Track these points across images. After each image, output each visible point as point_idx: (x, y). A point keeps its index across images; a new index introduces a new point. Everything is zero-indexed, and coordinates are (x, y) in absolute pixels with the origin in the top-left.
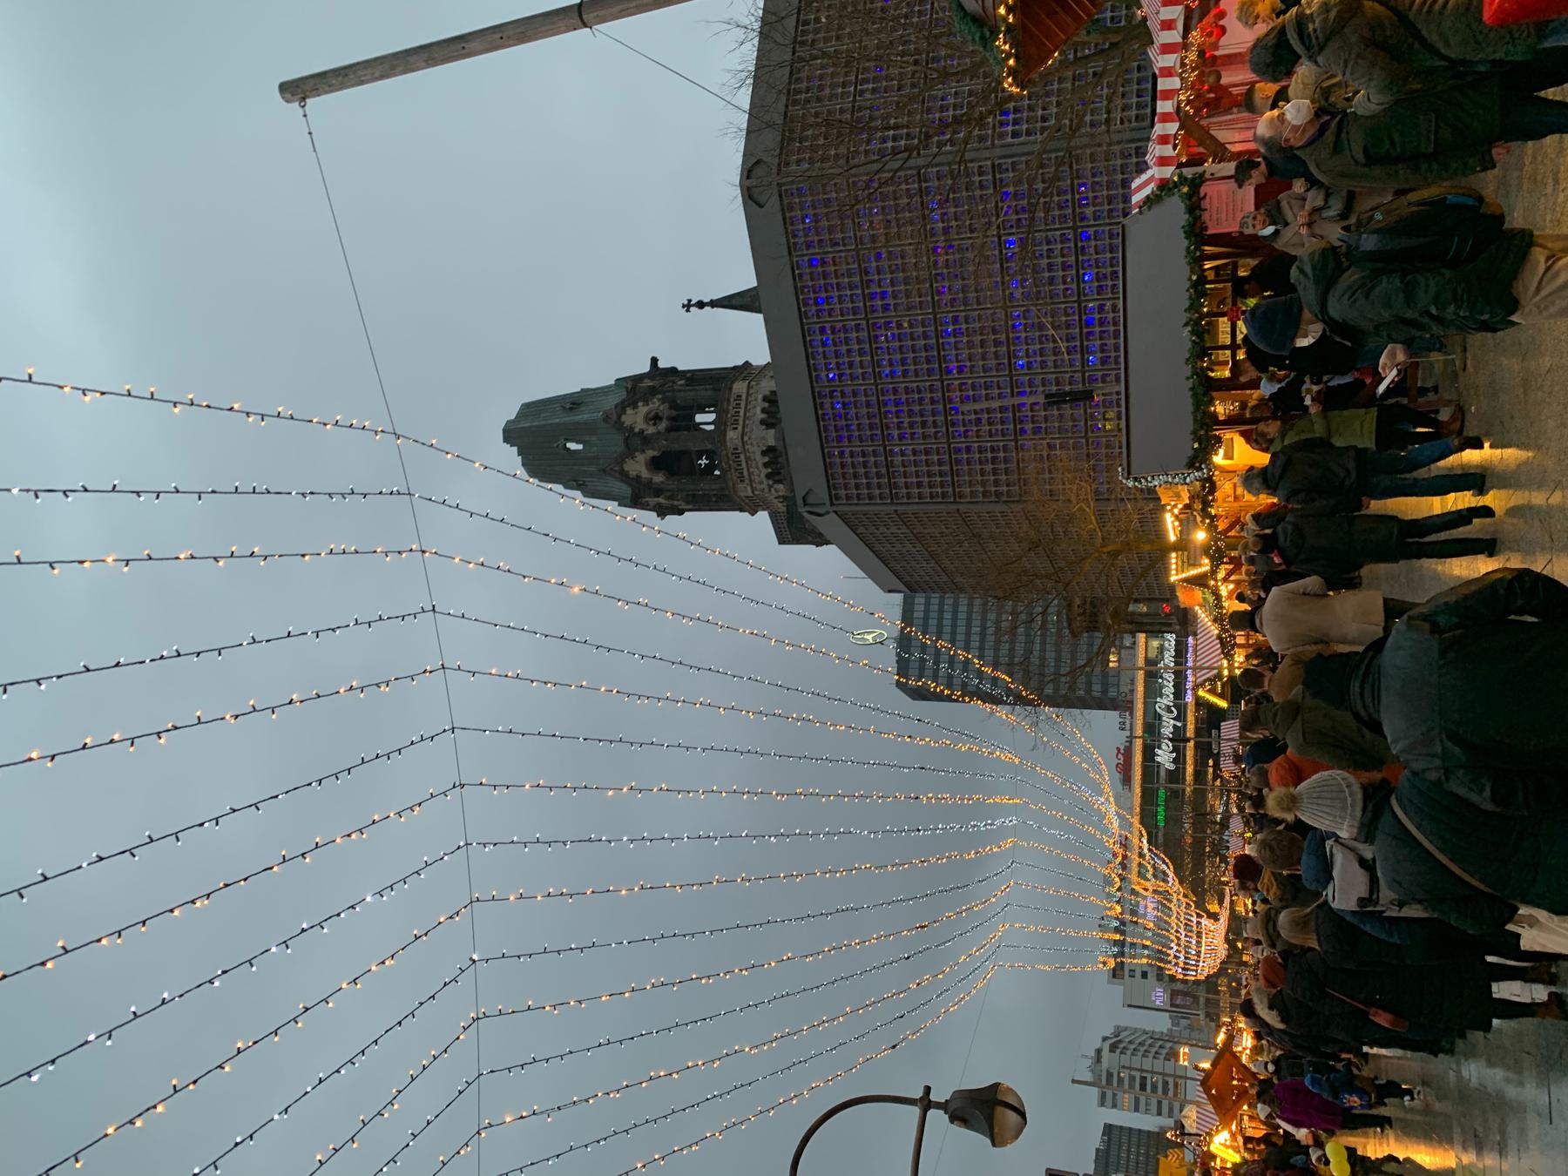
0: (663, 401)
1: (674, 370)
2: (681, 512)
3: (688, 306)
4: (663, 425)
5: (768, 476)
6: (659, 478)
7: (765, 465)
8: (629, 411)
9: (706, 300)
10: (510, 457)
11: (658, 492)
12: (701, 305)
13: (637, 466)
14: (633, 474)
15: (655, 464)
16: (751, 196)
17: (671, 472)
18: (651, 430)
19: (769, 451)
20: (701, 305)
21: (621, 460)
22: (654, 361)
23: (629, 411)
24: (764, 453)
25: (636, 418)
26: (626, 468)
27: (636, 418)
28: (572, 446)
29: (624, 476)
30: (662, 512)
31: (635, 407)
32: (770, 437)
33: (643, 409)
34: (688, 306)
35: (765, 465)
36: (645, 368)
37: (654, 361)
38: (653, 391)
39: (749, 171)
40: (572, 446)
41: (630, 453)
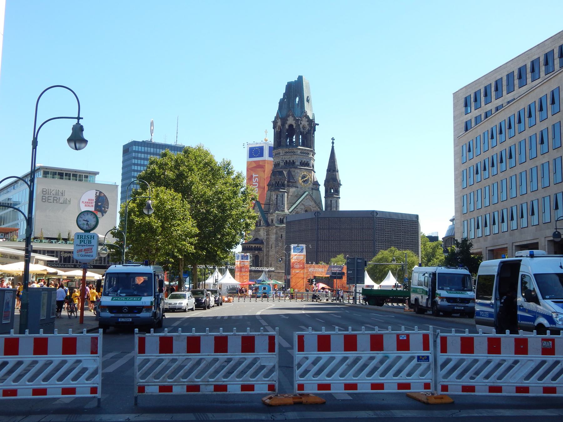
0: (308, 130)
1: (314, 130)
2: (274, 128)
3: (333, 139)
4: (302, 130)
5: (286, 161)
6: (287, 127)
7: (290, 161)
8: (307, 119)
9: (334, 145)
10: (294, 78)
11: (283, 124)
12: (333, 143)
13: (291, 121)
14: (288, 118)
15: (291, 126)
16: (373, 212)
17: (287, 131)
18: (301, 126)
19: (294, 163)
20: (333, 143)
21: (293, 116)
22: (318, 125)
23: (307, 119)
24: (293, 161)
25: (304, 122)
26: (291, 117)
27: (304, 122)
28: (297, 99)
29: (288, 116)
30: (275, 123)
31: (307, 121)
32: (298, 163)
33: (306, 124)
34: (333, 139)
35: (290, 161)
36: (316, 122)
37: (318, 125)
38: (311, 127)
39: (377, 212)
40: (297, 99)
41: (295, 119)
